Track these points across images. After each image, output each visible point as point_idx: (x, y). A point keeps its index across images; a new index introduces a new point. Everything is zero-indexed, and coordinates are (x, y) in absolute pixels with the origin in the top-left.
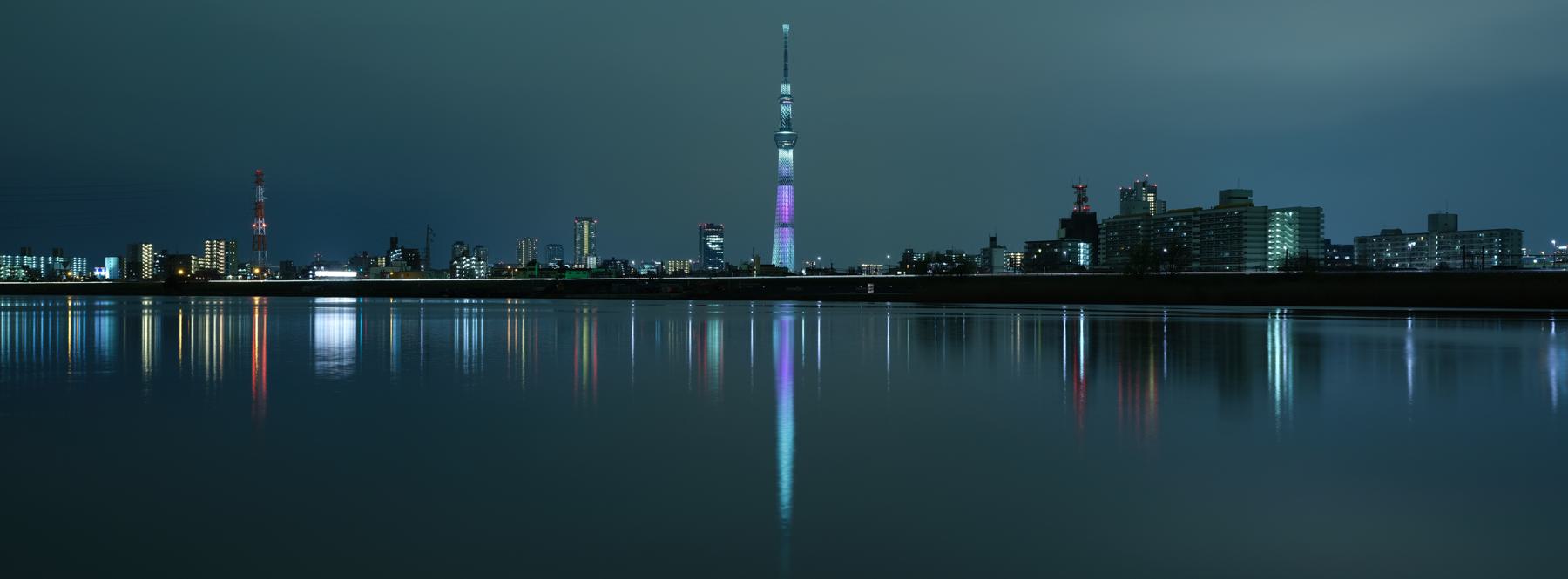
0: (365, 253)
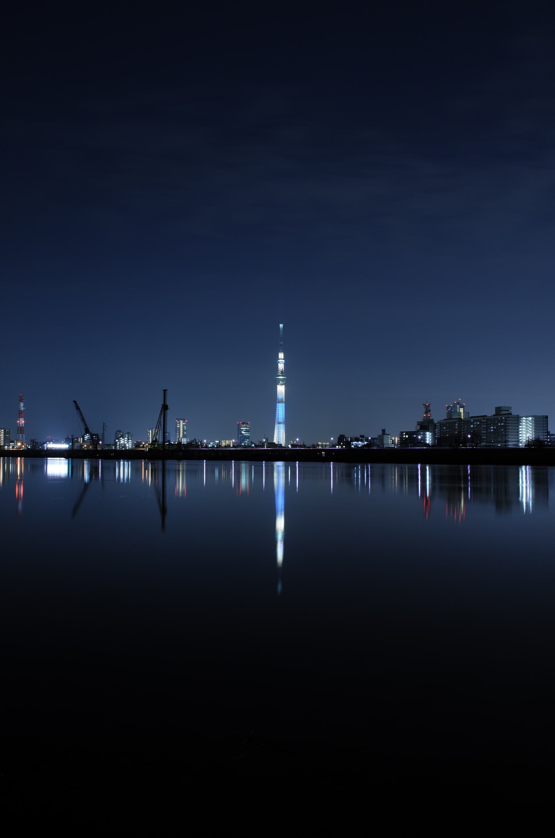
0: (72, 436)
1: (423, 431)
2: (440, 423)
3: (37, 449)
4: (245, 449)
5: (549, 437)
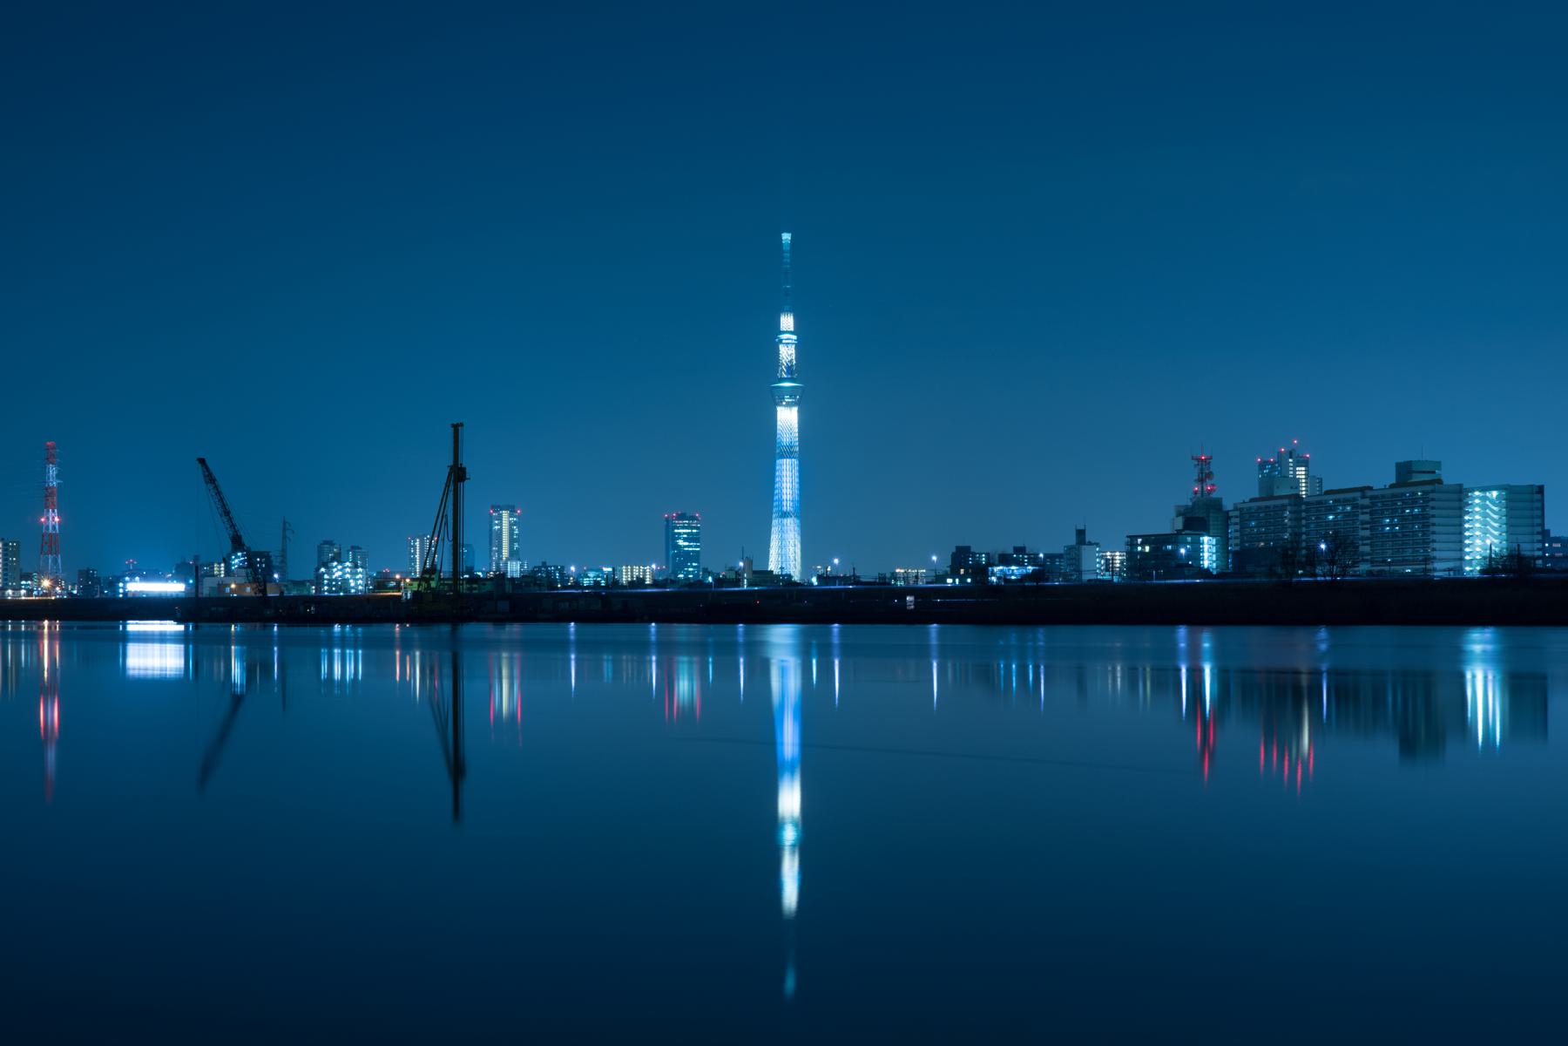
0: (196, 558)
2: (1241, 510)
3: (98, 596)
5: (1547, 545)
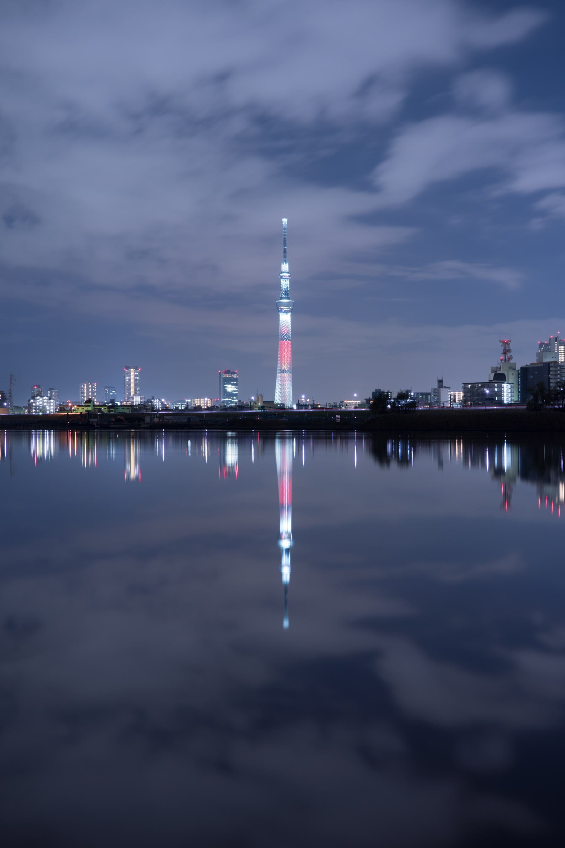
1: (498, 381)
4: (224, 411)
